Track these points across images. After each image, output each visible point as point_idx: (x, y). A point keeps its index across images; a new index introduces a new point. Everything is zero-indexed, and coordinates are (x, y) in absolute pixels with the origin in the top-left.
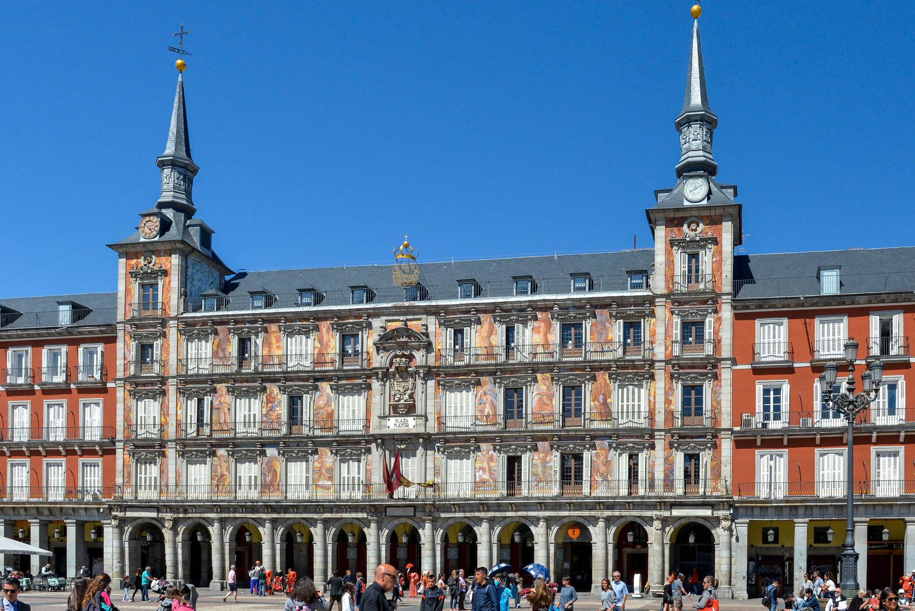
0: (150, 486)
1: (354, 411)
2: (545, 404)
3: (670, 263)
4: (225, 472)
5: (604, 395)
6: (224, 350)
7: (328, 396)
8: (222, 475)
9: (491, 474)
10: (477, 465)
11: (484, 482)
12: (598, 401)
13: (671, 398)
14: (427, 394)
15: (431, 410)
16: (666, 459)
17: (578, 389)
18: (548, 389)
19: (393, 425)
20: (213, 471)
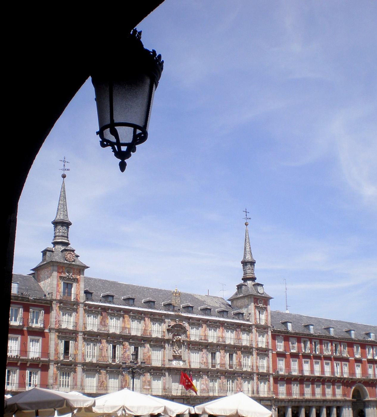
0: (63, 385)
1: (157, 356)
2: (222, 360)
3: (255, 313)
4: (104, 380)
5: (239, 358)
6: (104, 322)
7: (148, 348)
8: (103, 382)
9: (206, 386)
10: (202, 382)
11: (204, 390)
12: (238, 360)
13: (257, 361)
14: (183, 352)
15: (186, 359)
16: (257, 383)
17: (232, 355)
18: (223, 354)
19: (175, 364)
20: (99, 379)
